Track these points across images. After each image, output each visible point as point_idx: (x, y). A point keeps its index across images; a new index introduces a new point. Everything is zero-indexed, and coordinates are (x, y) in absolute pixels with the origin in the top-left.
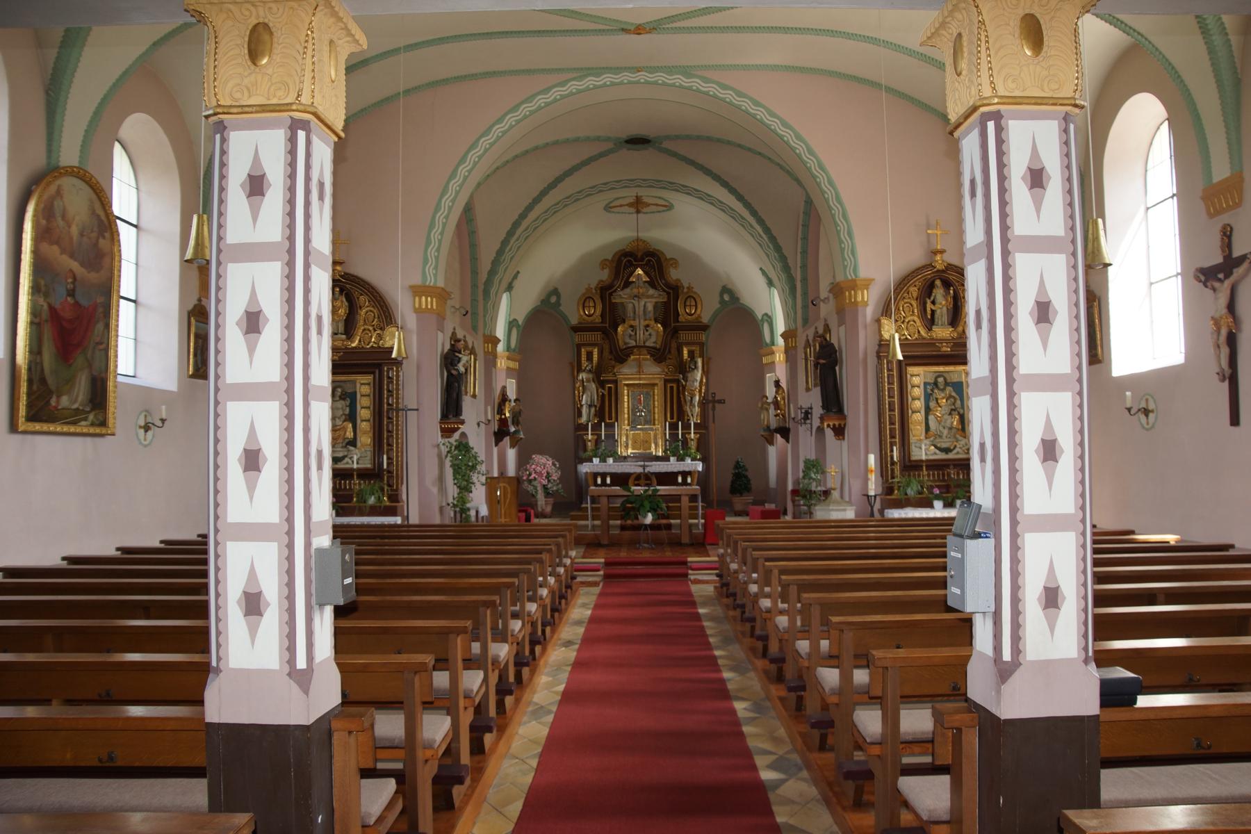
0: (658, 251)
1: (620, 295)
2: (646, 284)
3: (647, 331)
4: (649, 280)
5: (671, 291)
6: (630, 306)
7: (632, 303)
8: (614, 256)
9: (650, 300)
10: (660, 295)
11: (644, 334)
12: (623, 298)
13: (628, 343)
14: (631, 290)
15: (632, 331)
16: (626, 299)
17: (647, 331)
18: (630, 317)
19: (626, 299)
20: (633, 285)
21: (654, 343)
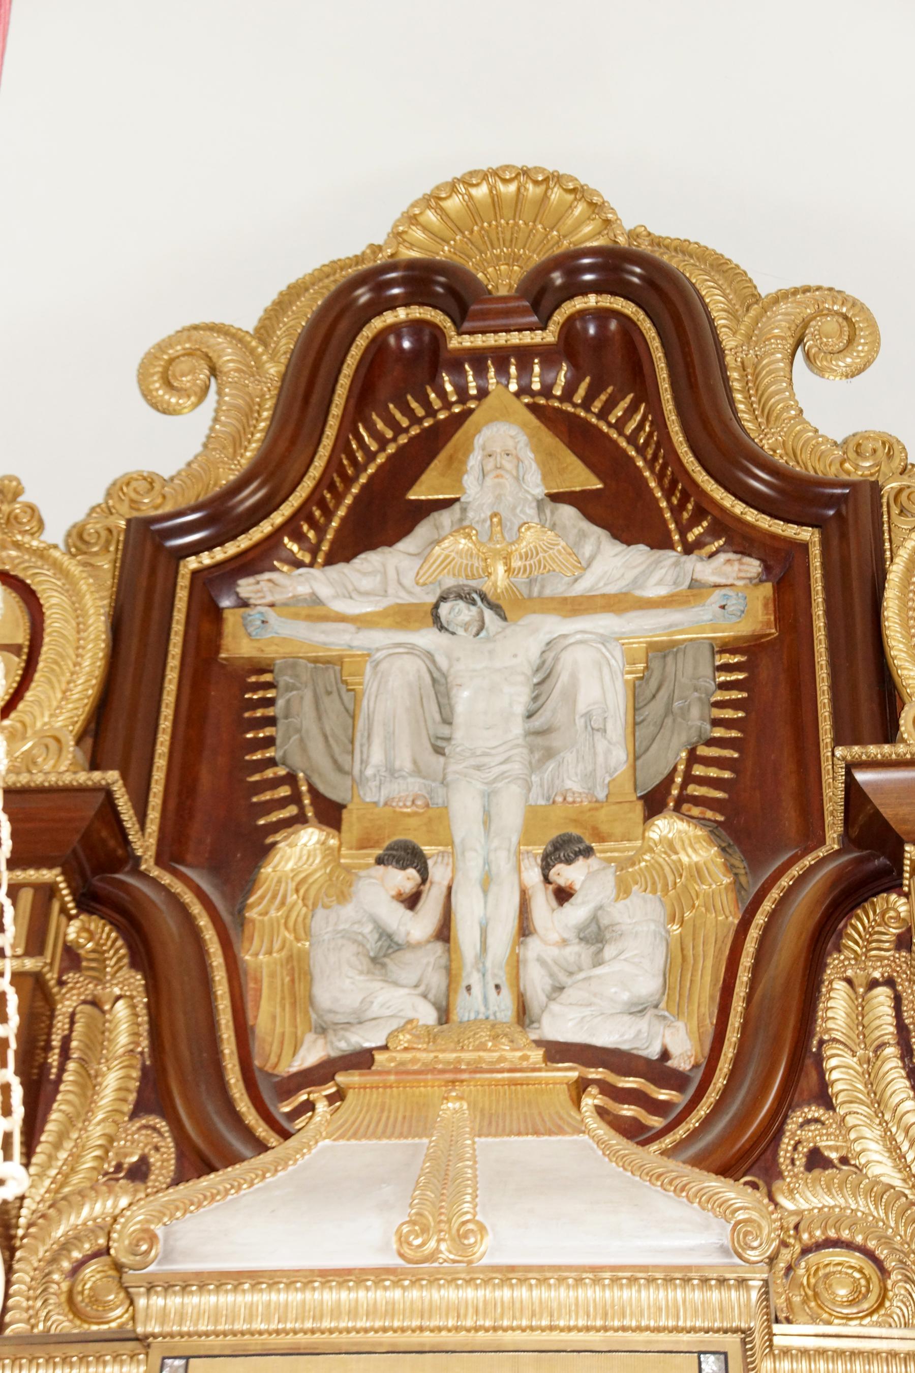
0: (682, 248)
1: (315, 600)
2: (568, 512)
3: (563, 895)
4: (600, 486)
5: (806, 534)
6: (413, 667)
7: (430, 656)
8: (281, 305)
9: (605, 623)
10: (694, 584)
11: (525, 929)
12: (342, 618)
13: (359, 1020)
14: (423, 555)
15: (412, 901)
16: (362, 622)
17: (563, 895)
18: (392, 772)
19: (362, 622)
20: (445, 518)
21: (638, 1009)
